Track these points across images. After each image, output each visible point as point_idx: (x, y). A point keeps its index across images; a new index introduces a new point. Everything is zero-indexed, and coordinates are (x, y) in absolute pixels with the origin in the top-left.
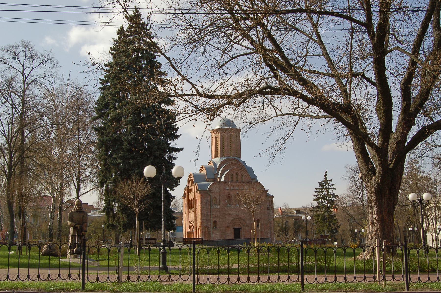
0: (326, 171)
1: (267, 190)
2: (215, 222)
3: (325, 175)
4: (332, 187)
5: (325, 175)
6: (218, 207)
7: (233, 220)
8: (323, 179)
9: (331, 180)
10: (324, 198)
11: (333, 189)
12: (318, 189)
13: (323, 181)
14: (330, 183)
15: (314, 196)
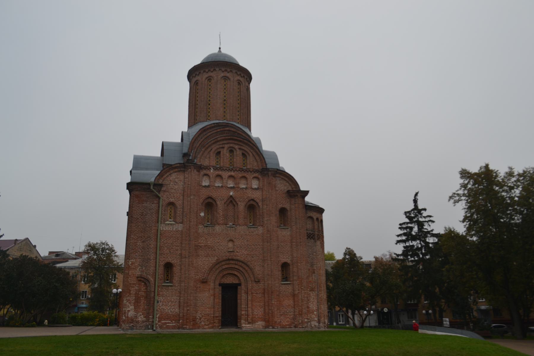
0: (416, 194)
1: (306, 193)
2: (169, 266)
3: (415, 201)
4: (427, 219)
5: (415, 201)
6: (180, 227)
7: (218, 263)
8: (412, 206)
9: (425, 210)
10: (414, 238)
11: (430, 223)
12: (404, 223)
13: (412, 210)
14: (425, 214)
15: (398, 236)
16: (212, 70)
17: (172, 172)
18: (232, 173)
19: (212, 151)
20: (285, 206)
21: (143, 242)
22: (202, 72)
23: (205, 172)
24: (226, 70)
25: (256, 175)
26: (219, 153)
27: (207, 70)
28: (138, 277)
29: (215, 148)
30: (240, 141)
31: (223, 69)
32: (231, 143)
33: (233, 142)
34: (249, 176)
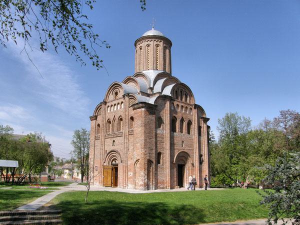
1: (208, 119)
16: (160, 41)
18: (182, 104)
25: (191, 107)
26: (176, 92)
27: (157, 40)
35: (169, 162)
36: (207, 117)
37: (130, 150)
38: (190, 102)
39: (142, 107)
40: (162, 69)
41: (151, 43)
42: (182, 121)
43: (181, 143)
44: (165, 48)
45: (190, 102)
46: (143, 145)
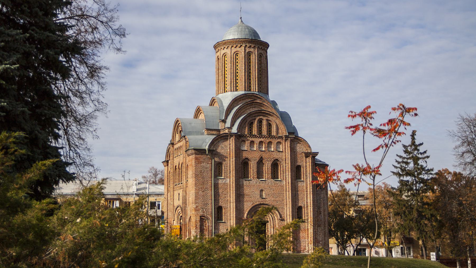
1: (316, 154)
10: (409, 173)
14: (422, 149)
16: (239, 45)
17: (219, 140)
18: (262, 139)
19: (247, 122)
20: (300, 164)
21: (203, 191)
22: (230, 46)
23: (243, 139)
24: (250, 47)
25: (279, 140)
27: (235, 46)
28: (201, 217)
29: (249, 120)
30: (267, 114)
31: (248, 45)
32: (261, 116)
33: (262, 114)
34: (275, 141)
35: (234, 219)
36: (313, 151)
37: (187, 206)
38: (277, 133)
39: (192, 154)
40: (243, 89)
41: (228, 51)
42: (260, 162)
43: (258, 193)
44: (248, 56)
45: (277, 133)
46: (194, 201)
